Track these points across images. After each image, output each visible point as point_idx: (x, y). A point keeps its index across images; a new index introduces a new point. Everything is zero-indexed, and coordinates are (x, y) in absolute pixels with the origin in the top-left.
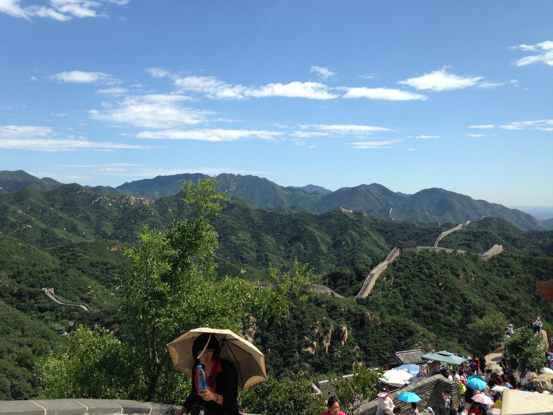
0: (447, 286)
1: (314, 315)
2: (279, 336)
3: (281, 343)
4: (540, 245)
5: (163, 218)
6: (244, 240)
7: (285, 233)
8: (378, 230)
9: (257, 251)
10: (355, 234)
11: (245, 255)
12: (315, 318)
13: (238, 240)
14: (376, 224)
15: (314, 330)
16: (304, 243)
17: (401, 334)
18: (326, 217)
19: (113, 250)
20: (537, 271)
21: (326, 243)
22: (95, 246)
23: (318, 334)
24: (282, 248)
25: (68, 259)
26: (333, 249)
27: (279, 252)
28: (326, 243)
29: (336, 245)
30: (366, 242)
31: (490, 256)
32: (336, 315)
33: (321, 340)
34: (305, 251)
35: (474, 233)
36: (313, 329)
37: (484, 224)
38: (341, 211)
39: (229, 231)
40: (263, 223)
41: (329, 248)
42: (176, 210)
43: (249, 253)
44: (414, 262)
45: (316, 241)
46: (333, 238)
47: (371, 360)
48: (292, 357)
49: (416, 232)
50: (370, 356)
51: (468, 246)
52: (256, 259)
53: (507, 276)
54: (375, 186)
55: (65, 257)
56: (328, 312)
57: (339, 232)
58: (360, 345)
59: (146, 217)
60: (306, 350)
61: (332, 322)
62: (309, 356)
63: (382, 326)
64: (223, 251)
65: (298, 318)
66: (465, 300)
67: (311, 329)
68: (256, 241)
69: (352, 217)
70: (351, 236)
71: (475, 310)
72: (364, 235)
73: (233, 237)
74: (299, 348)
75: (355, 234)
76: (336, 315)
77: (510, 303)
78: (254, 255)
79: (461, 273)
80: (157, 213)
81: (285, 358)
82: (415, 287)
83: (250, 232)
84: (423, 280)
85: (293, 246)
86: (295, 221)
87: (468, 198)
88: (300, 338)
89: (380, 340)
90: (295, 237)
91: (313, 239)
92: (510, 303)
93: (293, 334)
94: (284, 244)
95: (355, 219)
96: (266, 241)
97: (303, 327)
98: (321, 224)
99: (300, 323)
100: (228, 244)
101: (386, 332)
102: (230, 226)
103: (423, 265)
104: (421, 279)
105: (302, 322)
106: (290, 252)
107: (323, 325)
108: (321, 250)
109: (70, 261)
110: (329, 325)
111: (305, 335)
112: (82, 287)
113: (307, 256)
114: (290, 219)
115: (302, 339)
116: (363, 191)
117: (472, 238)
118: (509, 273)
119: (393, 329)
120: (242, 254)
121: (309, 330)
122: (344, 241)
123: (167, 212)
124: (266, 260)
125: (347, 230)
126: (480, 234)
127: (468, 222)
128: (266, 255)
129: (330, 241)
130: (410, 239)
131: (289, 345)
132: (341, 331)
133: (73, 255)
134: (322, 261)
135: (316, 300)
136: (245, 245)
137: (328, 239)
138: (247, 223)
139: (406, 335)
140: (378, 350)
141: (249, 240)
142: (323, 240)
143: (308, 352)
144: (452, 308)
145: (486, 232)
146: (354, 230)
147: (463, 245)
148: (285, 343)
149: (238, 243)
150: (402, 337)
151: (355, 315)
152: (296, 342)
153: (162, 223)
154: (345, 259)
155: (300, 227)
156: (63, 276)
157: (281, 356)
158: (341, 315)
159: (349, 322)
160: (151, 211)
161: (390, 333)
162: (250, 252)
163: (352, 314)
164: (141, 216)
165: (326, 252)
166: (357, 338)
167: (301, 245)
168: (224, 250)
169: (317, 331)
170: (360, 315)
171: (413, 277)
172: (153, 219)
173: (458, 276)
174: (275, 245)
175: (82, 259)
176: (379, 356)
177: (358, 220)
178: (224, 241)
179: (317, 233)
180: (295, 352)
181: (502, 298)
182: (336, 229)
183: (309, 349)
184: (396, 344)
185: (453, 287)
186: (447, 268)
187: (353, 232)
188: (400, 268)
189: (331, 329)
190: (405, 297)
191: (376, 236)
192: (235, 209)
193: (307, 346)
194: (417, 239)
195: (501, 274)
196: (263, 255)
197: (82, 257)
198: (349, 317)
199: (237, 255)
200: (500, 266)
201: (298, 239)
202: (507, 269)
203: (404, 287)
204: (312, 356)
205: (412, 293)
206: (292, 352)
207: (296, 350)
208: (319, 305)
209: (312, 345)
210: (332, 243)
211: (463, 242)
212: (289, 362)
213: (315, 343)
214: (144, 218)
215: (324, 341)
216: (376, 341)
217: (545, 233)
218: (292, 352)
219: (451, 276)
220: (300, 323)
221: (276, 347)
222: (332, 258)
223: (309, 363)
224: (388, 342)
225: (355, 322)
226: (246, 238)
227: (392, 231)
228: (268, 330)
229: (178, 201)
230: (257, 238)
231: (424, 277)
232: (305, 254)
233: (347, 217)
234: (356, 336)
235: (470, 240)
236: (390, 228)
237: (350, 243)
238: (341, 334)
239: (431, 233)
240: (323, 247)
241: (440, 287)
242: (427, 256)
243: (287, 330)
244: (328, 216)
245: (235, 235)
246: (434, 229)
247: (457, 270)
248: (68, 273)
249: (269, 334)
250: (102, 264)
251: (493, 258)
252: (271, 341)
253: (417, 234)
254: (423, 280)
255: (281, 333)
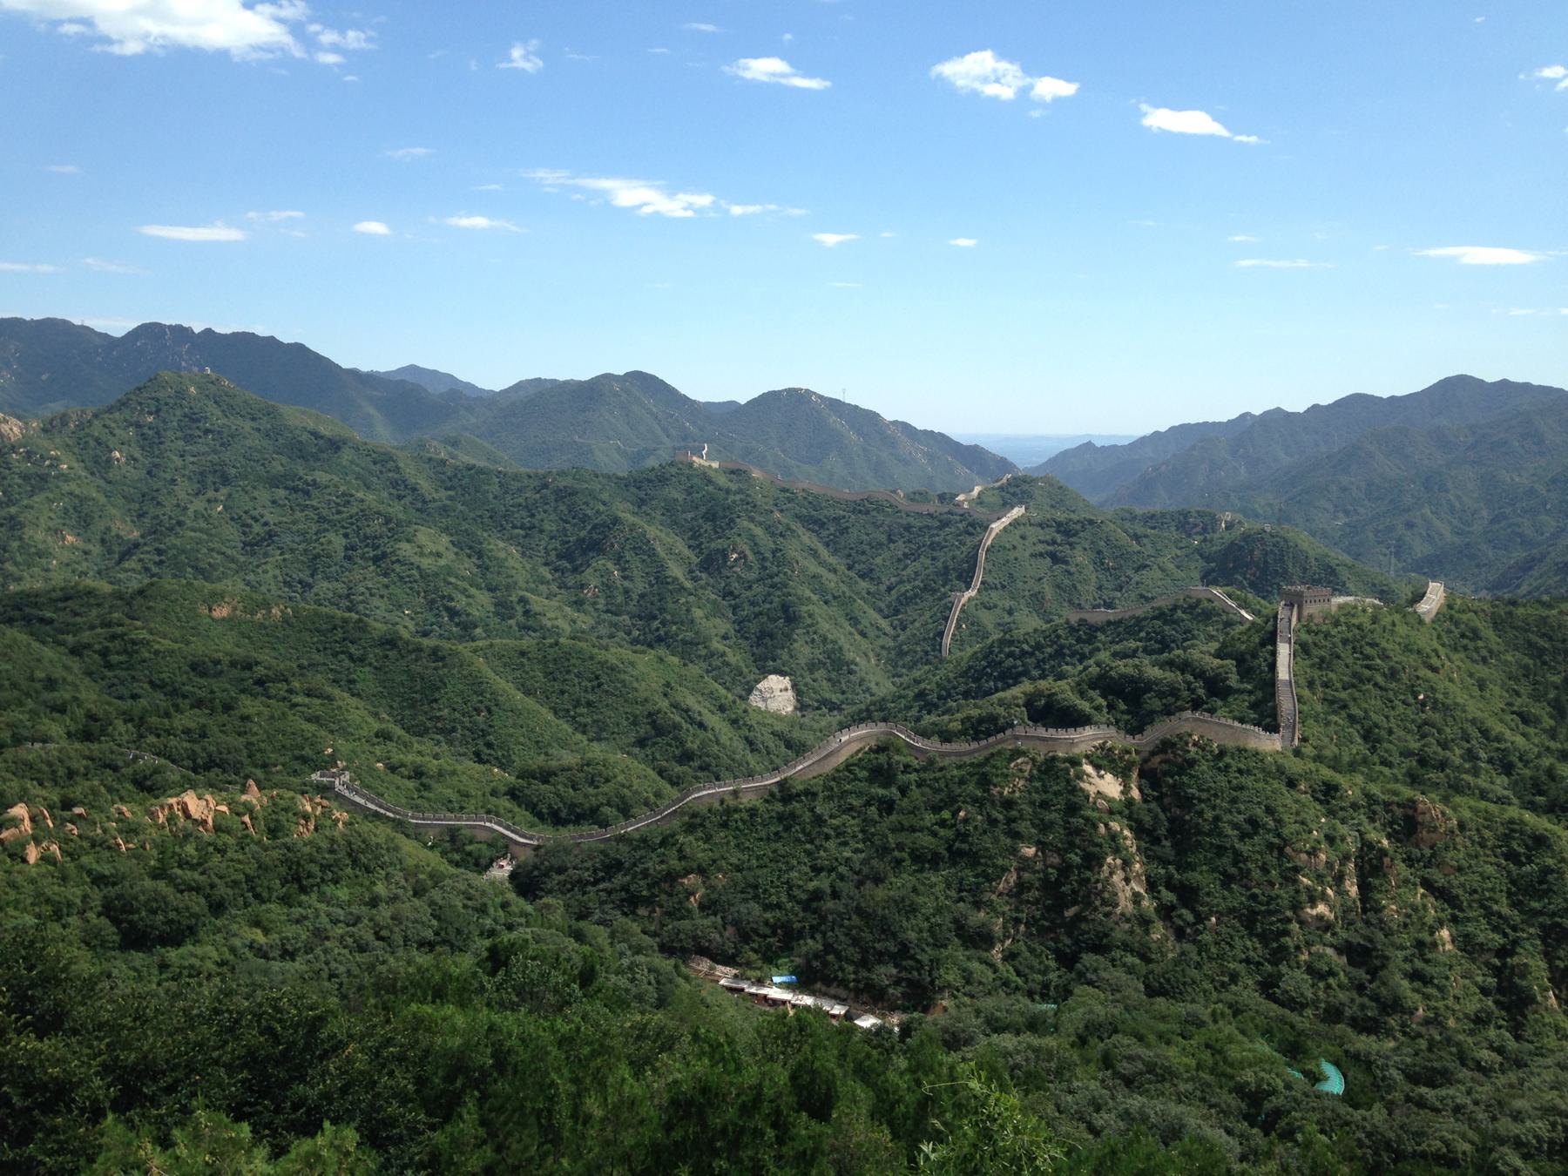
0: (1436, 701)
1: (1298, 814)
2: (1227, 881)
3: (1237, 897)
4: (1198, 551)
5: (102, 483)
6: (439, 555)
7: (542, 531)
8: (797, 516)
9: (491, 589)
10: (758, 531)
11: (460, 602)
12: (1303, 823)
13: (422, 554)
14: (790, 500)
15: (1316, 856)
16: (619, 559)
17: (1515, 845)
18: (650, 481)
19: (217, 614)
20: (1530, 644)
21: (680, 559)
22: (162, 606)
23: (1329, 865)
24: (549, 577)
25: (104, 653)
26: (704, 575)
27: (543, 588)
28: (680, 559)
29: (712, 563)
30: (792, 549)
31: (1434, 612)
32: (1342, 809)
33: (1339, 879)
34: (626, 583)
35: (1059, 524)
36: (1313, 853)
37: (1014, 494)
38: (691, 465)
39: (376, 526)
40: (450, 498)
41: (691, 572)
42: (137, 455)
43: (469, 596)
44: (1345, 642)
45: (652, 553)
46: (692, 542)
47: (1468, 919)
48: (1286, 933)
49: (904, 522)
50: (1462, 911)
51: (1055, 559)
52: (497, 614)
53: (1484, 660)
54: (644, 384)
55: (88, 646)
56: (1321, 802)
57: (708, 526)
58: (1427, 884)
59: (43, 478)
60: (1314, 912)
61: (1343, 829)
62: (1325, 926)
63: (1462, 826)
64: (385, 592)
65: (1264, 826)
66: (1485, 733)
67: (1308, 853)
68: (469, 556)
69: (722, 481)
70: (752, 537)
71: (1521, 759)
72: (781, 535)
73: (405, 546)
74: (1296, 907)
75: (758, 531)
76: (1342, 809)
77: (1544, 731)
78: (484, 599)
79: (1434, 661)
80: (75, 465)
81: (1264, 938)
82: (1371, 705)
83: (446, 530)
84: (1381, 688)
85: (590, 570)
86: (563, 494)
87: (872, 417)
88: (1290, 876)
89: (1470, 867)
90: (582, 540)
91: (643, 548)
92: (1544, 731)
93: (1265, 870)
94: (546, 564)
95: (734, 487)
96: (502, 555)
97: (1288, 850)
98: (641, 503)
99: (1276, 841)
100: (397, 567)
101: (1473, 842)
102: (378, 513)
103: (1368, 650)
104: (1376, 685)
105: (1279, 835)
106: (582, 586)
107: (1330, 839)
108: (676, 579)
109: (115, 658)
110: (1343, 839)
111: (1296, 870)
112: (307, 752)
113: (635, 597)
114: (545, 486)
115: (1295, 881)
116: (616, 395)
117: (1059, 538)
118: (1484, 653)
119: (1487, 834)
120: (451, 599)
121: (1304, 856)
122: (734, 550)
123: (109, 461)
124: (526, 613)
125: (732, 520)
126: (1078, 527)
127: (977, 489)
128: (522, 600)
129: (687, 552)
130: (891, 541)
131: (1268, 903)
132: (1383, 853)
133: (114, 637)
134: (698, 613)
135: (1281, 770)
136: (450, 571)
137: (681, 546)
138: (400, 498)
139: (1527, 847)
140: (1475, 891)
141: (452, 556)
142: (670, 551)
143: (1320, 918)
144: (1471, 756)
145: (1091, 522)
146: (752, 519)
147: (1041, 555)
148: (1254, 897)
149: (426, 563)
150: (1519, 854)
151: (1387, 805)
152: (1284, 894)
153: (103, 500)
154: (752, 604)
155: (589, 512)
156: (237, 723)
157: (1251, 934)
158: (1355, 806)
159: (1377, 824)
160: (56, 458)
161: (1483, 846)
162: (473, 591)
163: (1376, 802)
164: (26, 477)
165: (688, 585)
166: (1411, 867)
167: (610, 565)
168: (387, 587)
169: (1323, 856)
170: (1399, 805)
171: (1361, 681)
172: (73, 487)
173: (1435, 670)
174: (528, 566)
175: (156, 653)
176: (1482, 906)
177: (740, 491)
178: (376, 560)
179: (652, 531)
180: (1289, 921)
181: (1525, 719)
182: (690, 516)
183: (1321, 908)
184: (1509, 873)
185: (1448, 702)
186: (1411, 651)
187: (752, 526)
188: (1322, 660)
189: (1352, 847)
190: (1367, 736)
191: (807, 538)
192: (346, 455)
193: (1313, 902)
194: (910, 541)
195: (1476, 656)
196: (514, 598)
197: (156, 647)
198: (1374, 813)
199: (433, 602)
200: (1463, 636)
201: (594, 547)
202: (1480, 644)
203: (1355, 711)
204: (1327, 927)
205: (1376, 726)
206: (1279, 921)
207: (1289, 913)
208: (1292, 784)
209: (1324, 897)
210: (696, 560)
211: (1041, 548)
212: (1283, 948)
213: (1329, 891)
214: (39, 481)
215: (1347, 883)
216: (1460, 869)
217: (1163, 515)
218: (1279, 921)
219: (1430, 674)
220: (1276, 841)
221: (1231, 911)
222: (714, 602)
223: (1332, 946)
224: (1490, 869)
225: (1391, 824)
226: (442, 549)
227: (836, 520)
228: (1183, 867)
229: (138, 426)
230: (470, 548)
231: (1380, 679)
232: (626, 591)
233: (710, 481)
234: (1409, 861)
235: (1054, 542)
236: (831, 513)
237: (748, 552)
238: (1387, 860)
239: (944, 524)
240: (676, 571)
241: (1423, 704)
242: (1365, 620)
243: (1246, 860)
244: (660, 478)
245: (408, 541)
246: (950, 513)
247: (1428, 657)
248: (245, 711)
249: (1196, 874)
250: (233, 664)
251: (1439, 617)
252: (1208, 894)
253: (908, 528)
254: (1381, 688)
255: (1233, 870)
